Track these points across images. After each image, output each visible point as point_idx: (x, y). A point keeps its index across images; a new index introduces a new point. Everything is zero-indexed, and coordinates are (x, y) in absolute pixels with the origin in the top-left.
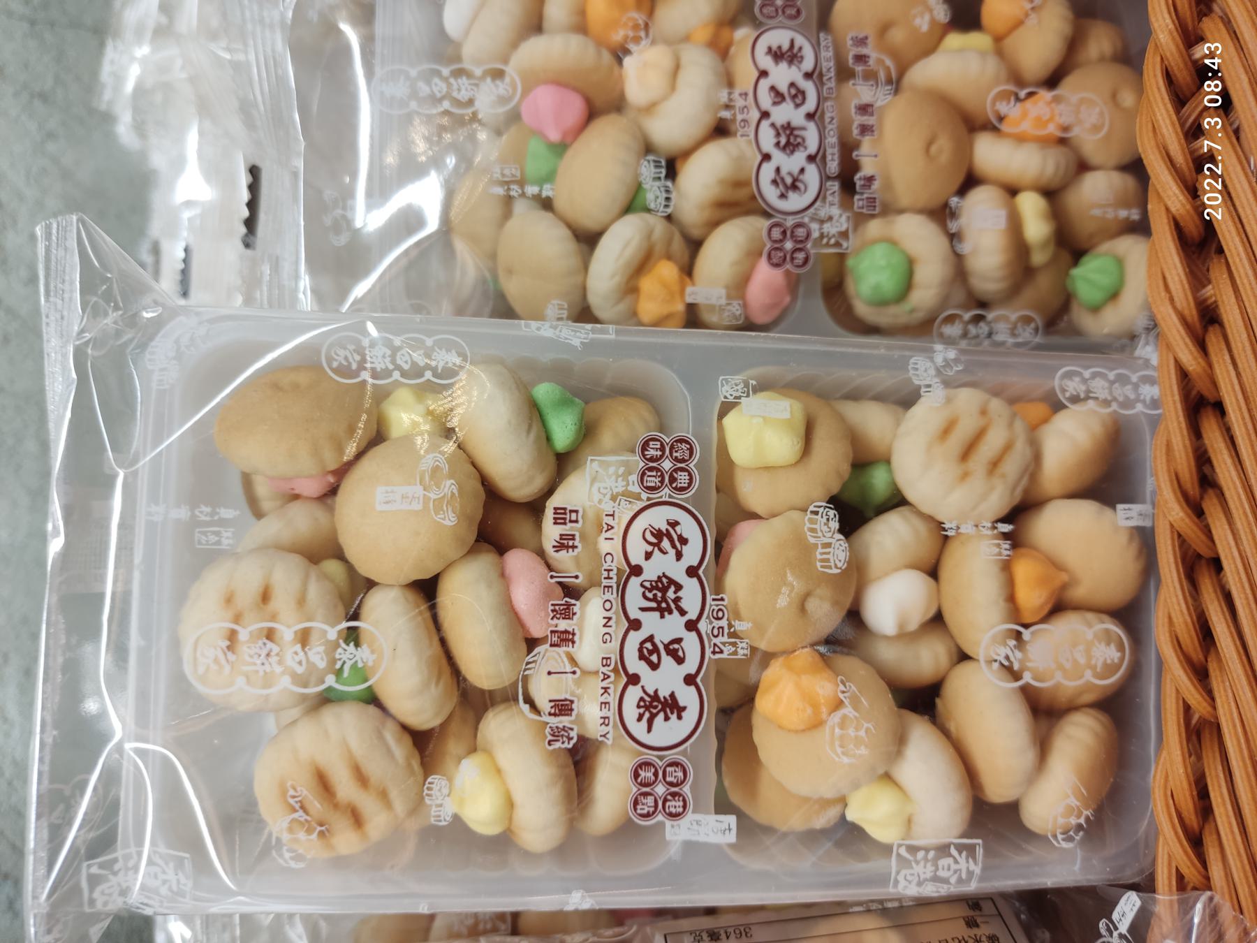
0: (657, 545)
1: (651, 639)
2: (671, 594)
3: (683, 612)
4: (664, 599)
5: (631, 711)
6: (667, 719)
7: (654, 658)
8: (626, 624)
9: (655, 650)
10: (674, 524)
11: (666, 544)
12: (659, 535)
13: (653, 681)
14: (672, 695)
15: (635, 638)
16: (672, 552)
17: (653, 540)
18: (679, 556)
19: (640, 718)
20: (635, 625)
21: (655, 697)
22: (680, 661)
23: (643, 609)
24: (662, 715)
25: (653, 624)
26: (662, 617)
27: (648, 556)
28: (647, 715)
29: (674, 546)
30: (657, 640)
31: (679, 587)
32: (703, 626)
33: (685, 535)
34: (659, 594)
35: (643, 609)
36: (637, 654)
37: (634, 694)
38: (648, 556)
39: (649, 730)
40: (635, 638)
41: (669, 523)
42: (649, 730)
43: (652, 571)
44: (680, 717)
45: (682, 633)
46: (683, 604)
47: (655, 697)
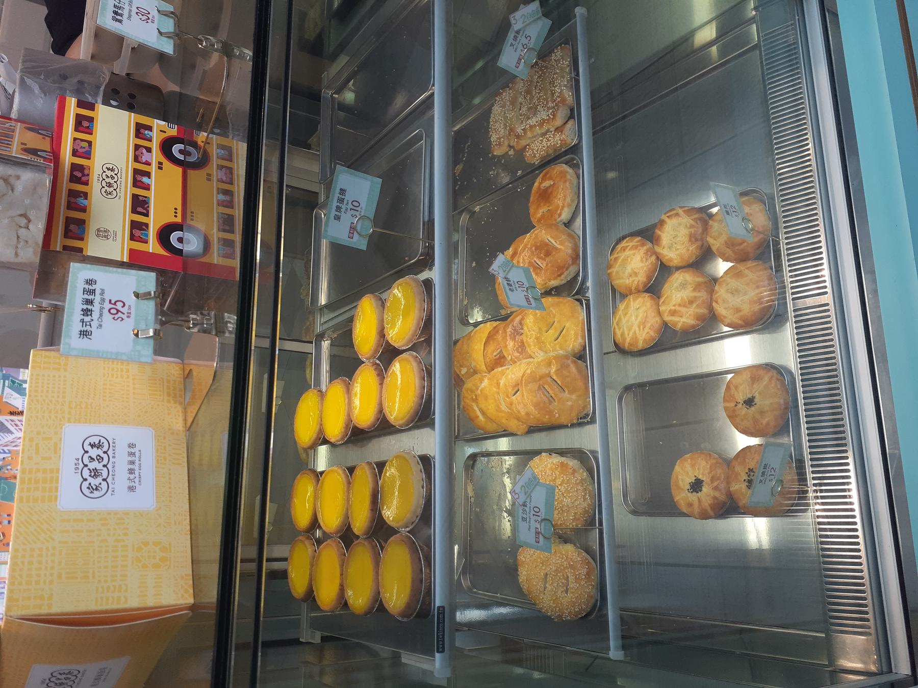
0: (97, 486)
1: (99, 462)
2: (93, 474)
3: (89, 469)
4: (95, 473)
5: (106, 444)
6: (94, 443)
7: (98, 458)
8: (107, 466)
9: (98, 460)
10: (92, 492)
11: (94, 487)
12: (96, 489)
13: (100, 452)
14: (92, 448)
15: (105, 462)
16: (92, 485)
17: (99, 488)
18: (90, 484)
19: (103, 443)
20: (105, 466)
21: (98, 448)
22: (90, 457)
23: (102, 470)
24: (96, 444)
25: (99, 466)
26: (96, 468)
27: (100, 484)
28: (101, 444)
29: (92, 487)
30: (98, 462)
31: (90, 476)
32: (81, 466)
33: (88, 490)
34: (97, 473)
35: (102, 470)
36: (104, 459)
37: (105, 449)
38: (100, 484)
39: (100, 441)
40: (105, 462)
41: (93, 493)
42: (100, 441)
43: (99, 480)
44: (90, 443)
45: (89, 464)
46: (89, 471)
47: (98, 448)
